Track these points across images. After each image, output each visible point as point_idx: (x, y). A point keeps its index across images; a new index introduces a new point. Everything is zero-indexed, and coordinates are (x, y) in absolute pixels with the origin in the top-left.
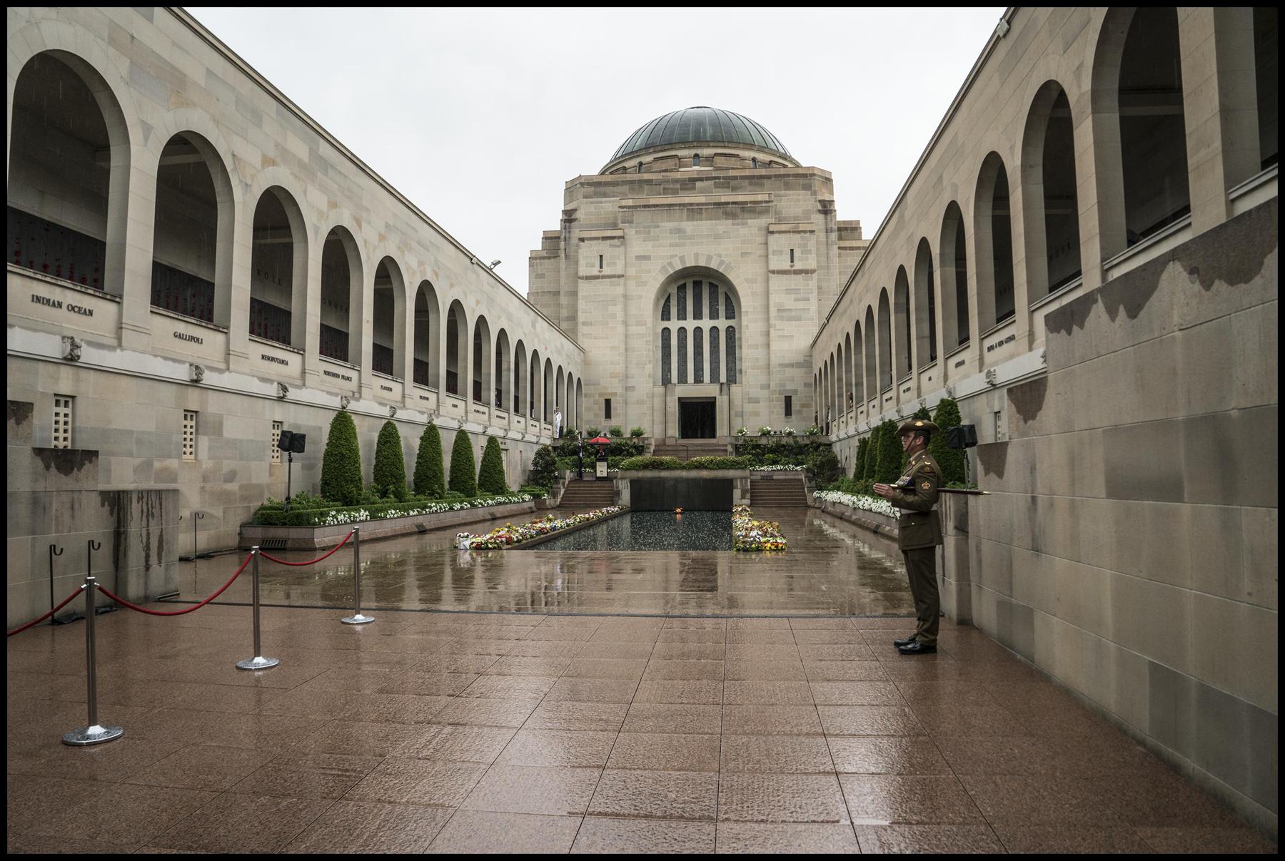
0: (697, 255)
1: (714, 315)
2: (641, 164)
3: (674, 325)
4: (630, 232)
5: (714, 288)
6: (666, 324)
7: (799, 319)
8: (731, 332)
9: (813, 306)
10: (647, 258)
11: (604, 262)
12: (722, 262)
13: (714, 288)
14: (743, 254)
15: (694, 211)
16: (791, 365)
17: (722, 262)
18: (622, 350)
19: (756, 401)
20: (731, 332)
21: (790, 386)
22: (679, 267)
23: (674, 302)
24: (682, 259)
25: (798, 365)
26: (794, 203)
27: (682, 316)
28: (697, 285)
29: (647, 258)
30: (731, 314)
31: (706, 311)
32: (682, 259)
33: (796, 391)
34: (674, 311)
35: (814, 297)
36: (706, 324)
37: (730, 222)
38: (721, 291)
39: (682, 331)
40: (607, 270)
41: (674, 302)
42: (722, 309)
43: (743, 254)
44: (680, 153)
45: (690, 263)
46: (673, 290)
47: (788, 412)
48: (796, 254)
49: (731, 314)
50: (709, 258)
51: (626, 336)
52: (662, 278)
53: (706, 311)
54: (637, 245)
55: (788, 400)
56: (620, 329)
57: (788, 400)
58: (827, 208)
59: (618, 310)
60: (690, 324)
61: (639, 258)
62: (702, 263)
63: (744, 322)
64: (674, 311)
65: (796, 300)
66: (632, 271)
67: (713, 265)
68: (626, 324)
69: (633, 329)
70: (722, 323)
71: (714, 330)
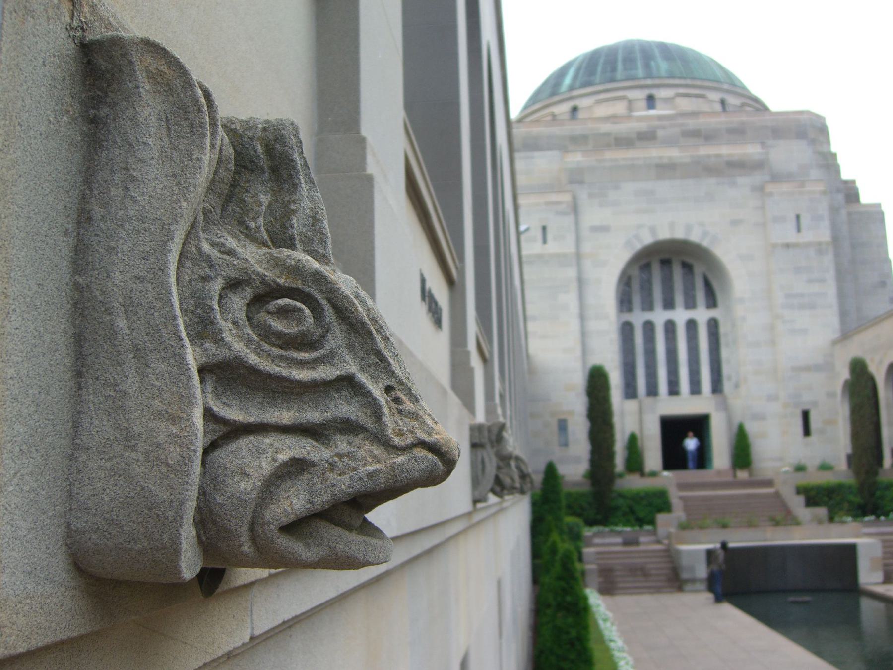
0: (672, 226)
1: (690, 304)
2: (575, 109)
3: (638, 318)
4: (583, 194)
5: (687, 267)
6: (627, 317)
7: (812, 306)
8: (713, 325)
9: (831, 289)
10: (603, 229)
11: (549, 236)
12: (705, 234)
13: (687, 267)
14: (735, 223)
15: (666, 170)
16: (807, 369)
17: (705, 234)
18: (578, 353)
19: (760, 417)
20: (713, 325)
21: (807, 399)
22: (648, 240)
23: (636, 285)
24: (653, 230)
25: (816, 368)
26: (788, 155)
27: (648, 306)
28: (666, 263)
29: (603, 229)
30: (712, 301)
31: (679, 298)
32: (653, 230)
33: (815, 404)
34: (637, 299)
35: (830, 276)
36: (680, 316)
37: (712, 181)
38: (699, 270)
39: (649, 327)
40: (552, 247)
41: (636, 285)
42: (700, 295)
43: (735, 223)
44: (632, 94)
45: (664, 234)
46: (635, 272)
47: (807, 432)
48: (804, 222)
49: (712, 301)
50: (689, 228)
51: (584, 334)
52: (625, 256)
53: (679, 298)
54: (593, 215)
55: (806, 416)
56: (574, 325)
57: (806, 416)
58: (829, 163)
59: (570, 299)
60: (659, 317)
61: (596, 229)
62: (679, 235)
63: (739, 310)
64: (637, 299)
65: (810, 281)
66: (587, 247)
67: (695, 237)
68: (582, 317)
69: (593, 325)
70: (702, 315)
71: (691, 325)
